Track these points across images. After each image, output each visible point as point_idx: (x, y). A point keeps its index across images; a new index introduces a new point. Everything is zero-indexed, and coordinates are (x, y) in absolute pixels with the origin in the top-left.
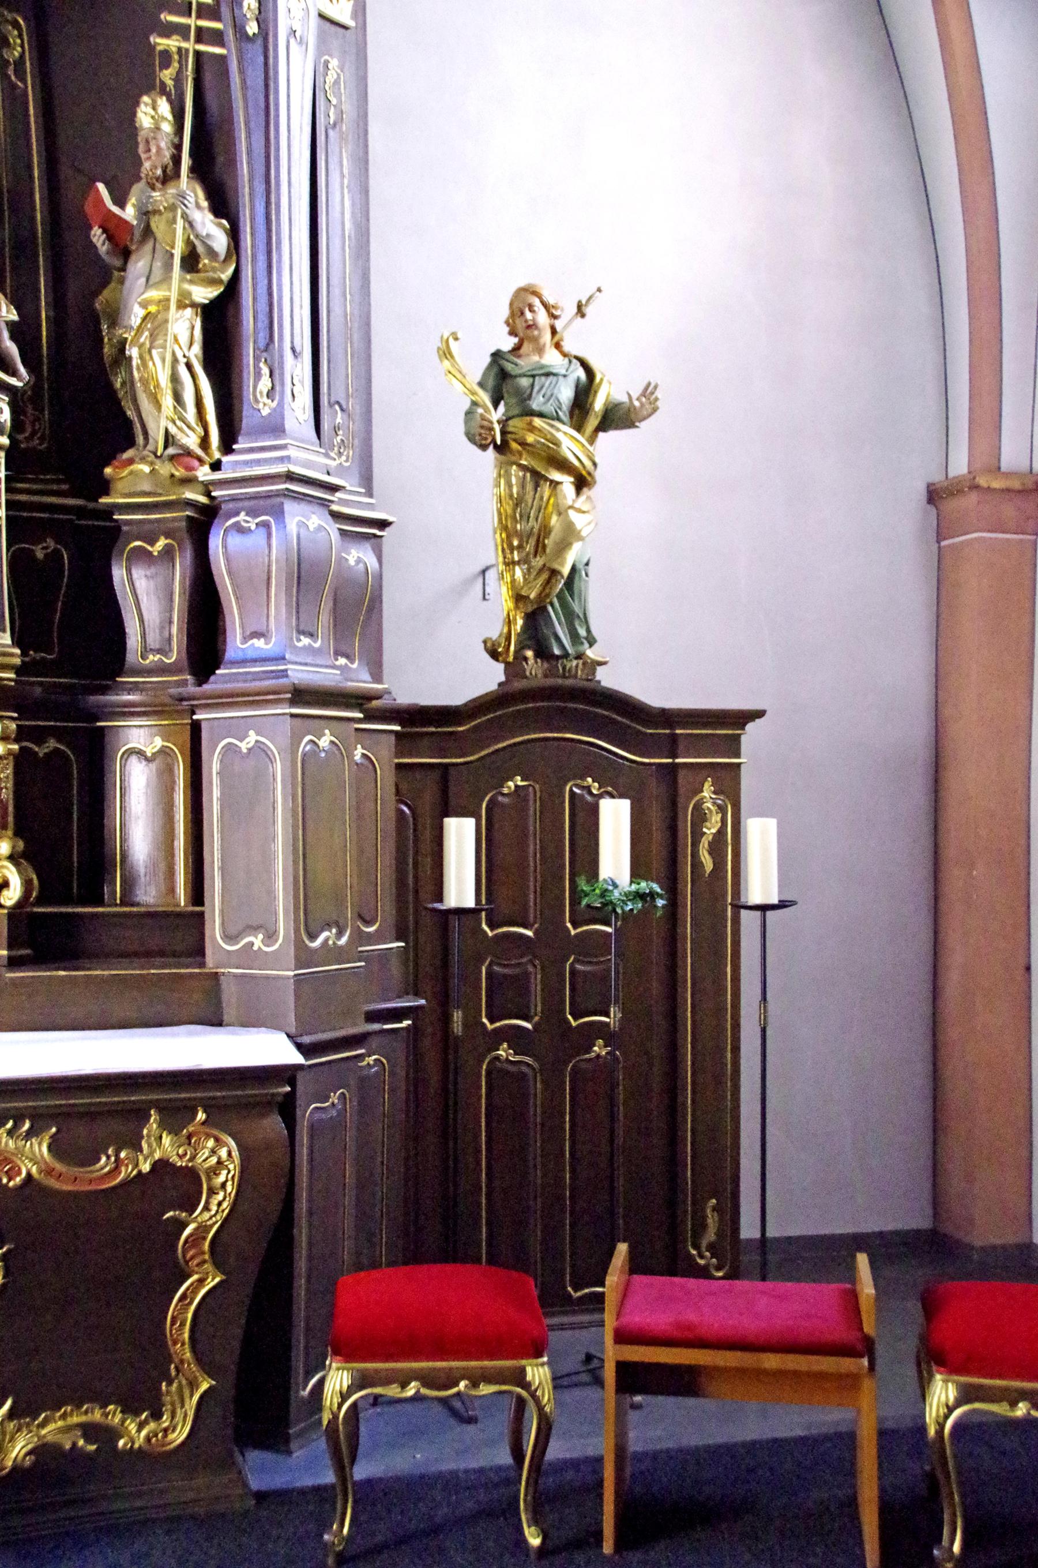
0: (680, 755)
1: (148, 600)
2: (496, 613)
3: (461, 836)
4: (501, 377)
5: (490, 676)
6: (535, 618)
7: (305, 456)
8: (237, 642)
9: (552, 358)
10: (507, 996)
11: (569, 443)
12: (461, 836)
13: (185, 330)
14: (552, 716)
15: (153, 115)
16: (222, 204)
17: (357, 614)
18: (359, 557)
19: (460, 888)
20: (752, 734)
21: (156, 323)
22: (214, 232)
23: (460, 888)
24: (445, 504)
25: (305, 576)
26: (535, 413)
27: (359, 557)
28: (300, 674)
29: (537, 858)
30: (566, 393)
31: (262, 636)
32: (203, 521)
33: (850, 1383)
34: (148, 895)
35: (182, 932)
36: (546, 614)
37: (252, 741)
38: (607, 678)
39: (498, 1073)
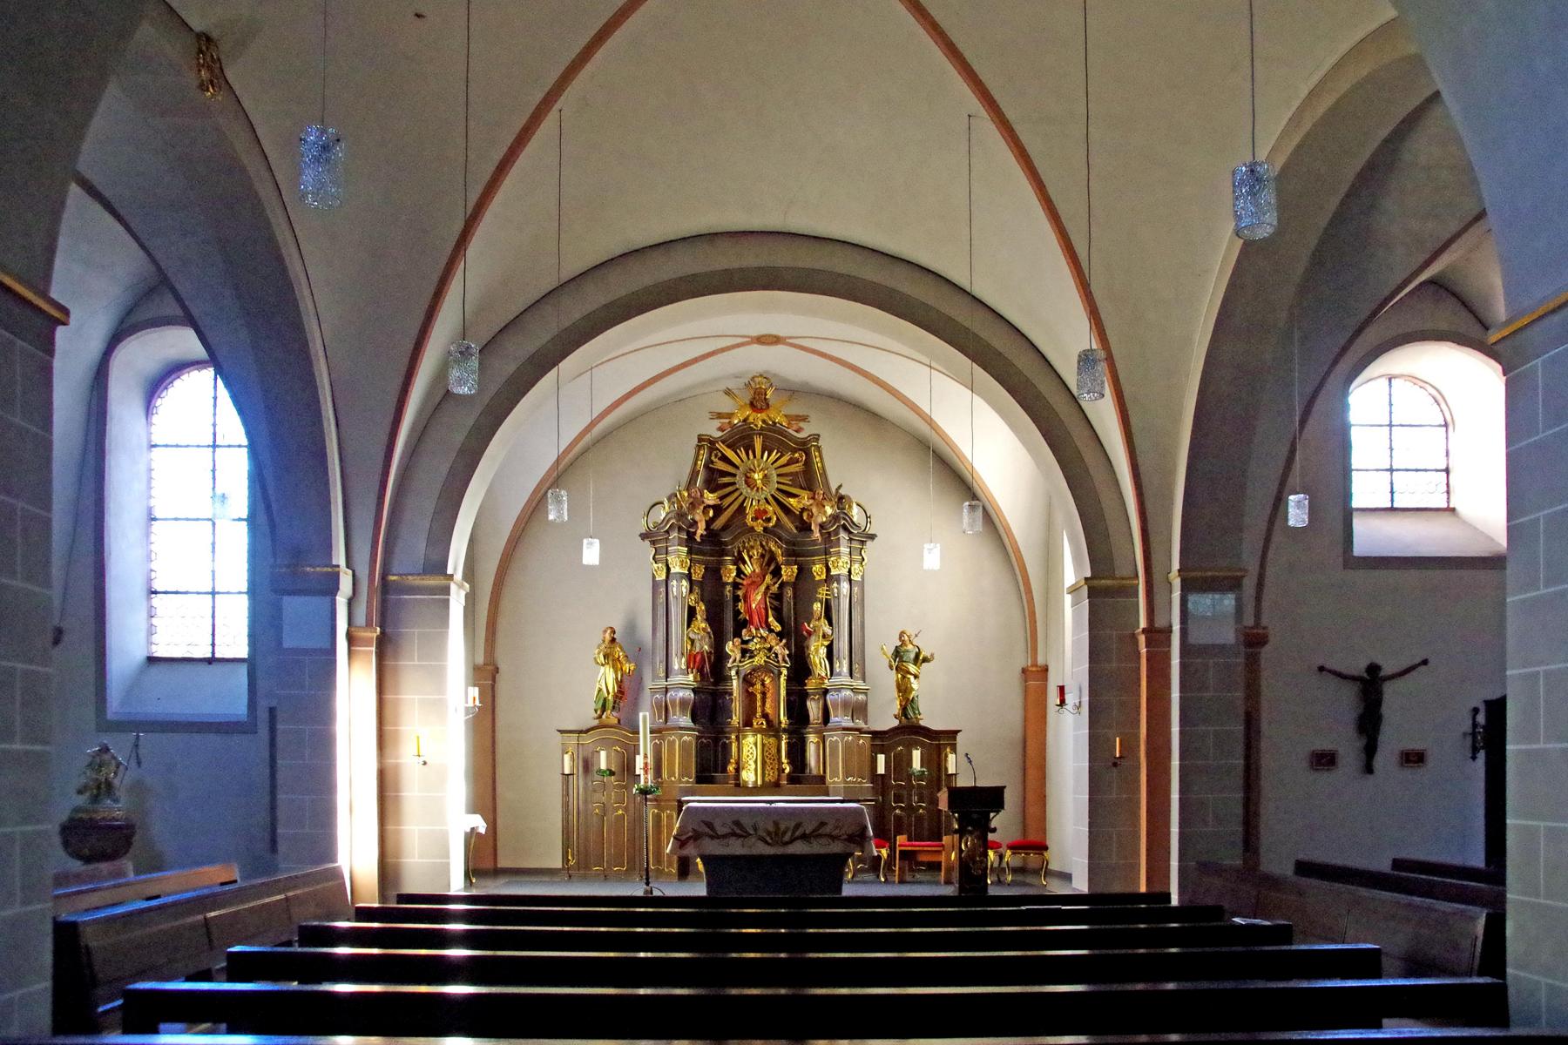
0: (939, 742)
1: (814, 709)
2: (896, 708)
3: (881, 758)
4: (898, 653)
5: (896, 723)
6: (904, 710)
7: (846, 680)
8: (833, 718)
9: (910, 647)
10: (898, 799)
11: (912, 668)
12: (881, 758)
13: (823, 651)
14: (910, 730)
15: (817, 607)
16: (831, 624)
17: (859, 710)
18: (861, 697)
19: (881, 770)
20: (959, 736)
21: (817, 650)
22: (828, 630)
23: (881, 770)
24: (884, 680)
25: (846, 704)
26: (904, 658)
27: (861, 697)
28: (844, 724)
29: (900, 765)
30: (912, 656)
31: (839, 719)
32: (826, 691)
33: (939, 852)
34: (815, 772)
35: (822, 779)
36: (908, 706)
37: (833, 738)
38: (922, 723)
39: (896, 816)
